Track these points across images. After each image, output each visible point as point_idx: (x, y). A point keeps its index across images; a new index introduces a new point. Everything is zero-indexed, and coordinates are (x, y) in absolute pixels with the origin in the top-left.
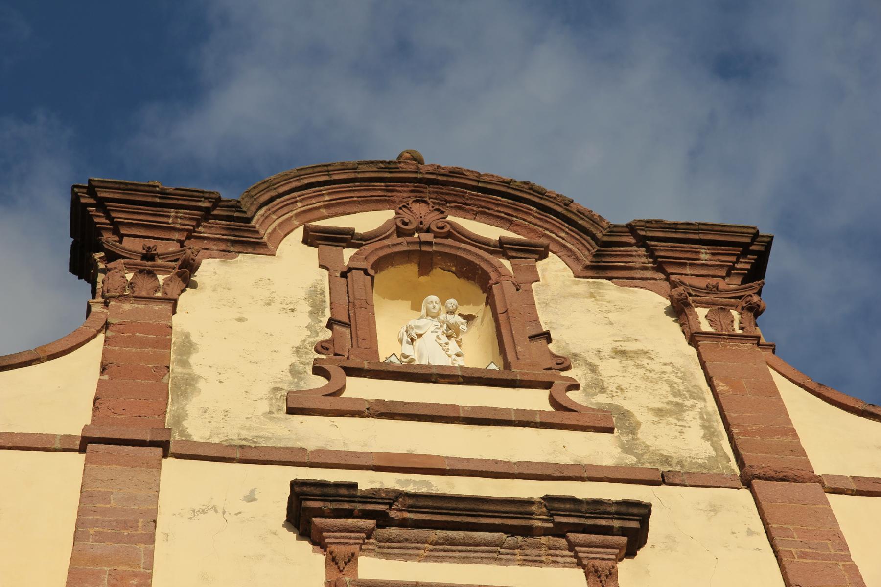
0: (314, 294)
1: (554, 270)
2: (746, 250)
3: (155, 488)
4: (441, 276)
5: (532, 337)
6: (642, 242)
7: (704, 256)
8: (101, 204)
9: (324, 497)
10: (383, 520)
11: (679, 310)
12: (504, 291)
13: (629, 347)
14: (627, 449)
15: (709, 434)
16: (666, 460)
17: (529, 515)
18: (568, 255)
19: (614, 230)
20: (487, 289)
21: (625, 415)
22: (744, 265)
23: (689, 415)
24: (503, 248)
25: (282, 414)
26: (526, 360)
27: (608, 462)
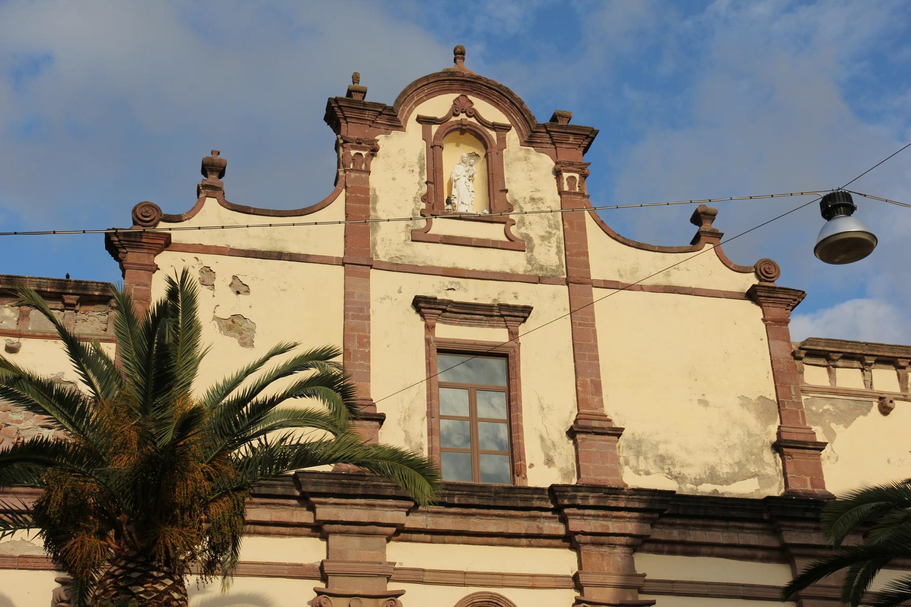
0: (421, 158)
1: (513, 137)
2: (588, 136)
3: (368, 288)
5: (501, 191)
6: (548, 132)
7: (571, 140)
8: (340, 107)
9: (426, 302)
10: (444, 311)
11: (558, 174)
13: (537, 195)
14: (529, 262)
16: (541, 268)
17: (492, 311)
18: (519, 130)
19: (538, 126)
20: (486, 147)
21: (530, 240)
22: (586, 143)
23: (553, 239)
24: (495, 127)
25: (409, 242)
26: (498, 207)
27: (521, 271)
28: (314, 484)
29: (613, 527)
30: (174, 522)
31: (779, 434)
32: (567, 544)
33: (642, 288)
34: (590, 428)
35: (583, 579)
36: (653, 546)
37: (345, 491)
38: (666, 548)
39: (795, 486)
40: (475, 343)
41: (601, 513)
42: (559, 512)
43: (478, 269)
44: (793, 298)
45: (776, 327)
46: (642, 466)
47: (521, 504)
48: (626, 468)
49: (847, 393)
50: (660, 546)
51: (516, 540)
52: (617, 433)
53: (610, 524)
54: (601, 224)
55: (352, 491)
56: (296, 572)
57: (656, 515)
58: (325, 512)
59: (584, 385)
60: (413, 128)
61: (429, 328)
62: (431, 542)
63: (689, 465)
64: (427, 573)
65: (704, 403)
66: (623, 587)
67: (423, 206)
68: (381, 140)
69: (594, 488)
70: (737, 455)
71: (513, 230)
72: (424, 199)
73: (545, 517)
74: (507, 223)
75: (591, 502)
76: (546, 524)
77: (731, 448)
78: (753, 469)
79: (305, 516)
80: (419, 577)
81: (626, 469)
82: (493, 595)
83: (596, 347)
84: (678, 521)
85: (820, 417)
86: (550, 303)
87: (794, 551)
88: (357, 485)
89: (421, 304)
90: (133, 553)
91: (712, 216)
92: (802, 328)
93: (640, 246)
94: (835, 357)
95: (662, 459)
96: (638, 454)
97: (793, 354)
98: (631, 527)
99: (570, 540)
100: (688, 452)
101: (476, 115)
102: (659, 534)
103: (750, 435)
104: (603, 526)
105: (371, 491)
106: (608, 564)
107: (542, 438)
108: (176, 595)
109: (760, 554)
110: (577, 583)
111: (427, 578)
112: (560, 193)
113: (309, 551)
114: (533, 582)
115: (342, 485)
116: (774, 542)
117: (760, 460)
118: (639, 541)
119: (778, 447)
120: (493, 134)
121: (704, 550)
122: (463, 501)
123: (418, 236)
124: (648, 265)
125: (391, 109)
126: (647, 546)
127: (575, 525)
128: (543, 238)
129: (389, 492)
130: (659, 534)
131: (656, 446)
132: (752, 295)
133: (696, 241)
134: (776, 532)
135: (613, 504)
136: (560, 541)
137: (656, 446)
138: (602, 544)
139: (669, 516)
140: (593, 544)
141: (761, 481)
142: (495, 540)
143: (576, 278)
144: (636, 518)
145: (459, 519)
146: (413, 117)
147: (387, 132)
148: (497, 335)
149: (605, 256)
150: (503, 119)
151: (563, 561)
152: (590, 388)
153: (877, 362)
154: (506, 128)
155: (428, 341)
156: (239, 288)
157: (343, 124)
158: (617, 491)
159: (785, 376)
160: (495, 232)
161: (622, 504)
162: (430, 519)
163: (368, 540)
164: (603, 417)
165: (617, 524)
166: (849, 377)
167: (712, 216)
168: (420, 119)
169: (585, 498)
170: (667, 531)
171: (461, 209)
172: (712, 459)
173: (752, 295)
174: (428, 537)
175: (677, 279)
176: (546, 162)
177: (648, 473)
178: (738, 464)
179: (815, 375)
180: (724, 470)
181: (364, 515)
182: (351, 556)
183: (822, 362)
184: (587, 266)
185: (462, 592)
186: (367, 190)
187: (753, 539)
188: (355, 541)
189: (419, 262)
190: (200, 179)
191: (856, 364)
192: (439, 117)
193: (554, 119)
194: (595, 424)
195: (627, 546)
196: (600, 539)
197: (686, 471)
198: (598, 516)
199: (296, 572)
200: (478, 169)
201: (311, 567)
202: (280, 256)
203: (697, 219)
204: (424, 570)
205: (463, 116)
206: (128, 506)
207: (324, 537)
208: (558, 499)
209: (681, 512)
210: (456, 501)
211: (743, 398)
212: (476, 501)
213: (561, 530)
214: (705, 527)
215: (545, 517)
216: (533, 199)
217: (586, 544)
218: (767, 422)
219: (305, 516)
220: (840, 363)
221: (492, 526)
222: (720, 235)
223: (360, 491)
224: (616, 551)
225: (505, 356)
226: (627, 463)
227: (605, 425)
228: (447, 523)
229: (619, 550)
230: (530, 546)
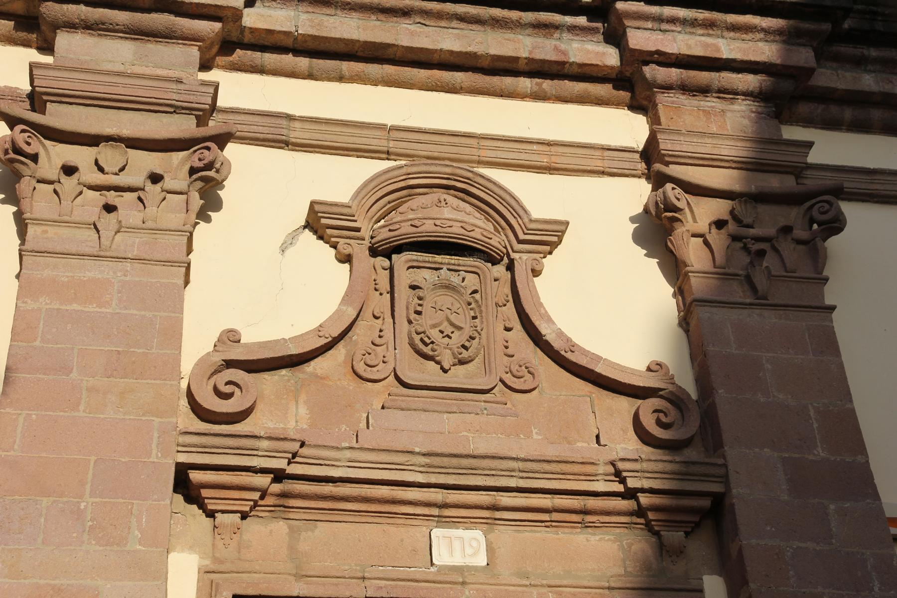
29: (727, 47)
32: (625, 95)
35: (666, 144)
36: (817, 109)
38: (848, 114)
50: (834, 110)
51: (508, 82)
53: (721, 43)
57: (826, 27)
62: (310, 76)
64: (297, 125)
73: (572, 29)
76: (575, 45)
80: (277, 133)
84: (874, 53)
98: (765, 51)
99: (630, 85)
102: (830, 78)
104: (706, 45)
110: (650, 153)
111: (297, 134)
118: (787, 86)
126: (804, 108)
127: (640, 39)
130: (830, 78)
136: (610, 86)
138: (704, 91)
139: (852, 37)
140: (686, 88)
144: (779, 32)
162: (304, 16)
165: (738, 44)
170: (848, 75)
174: (303, 63)
198: (693, 23)
204: (290, 118)
209: (879, 26)
213: (610, 57)
215: (572, 29)
217: (667, 87)
224: (736, 107)
230: (539, 96)
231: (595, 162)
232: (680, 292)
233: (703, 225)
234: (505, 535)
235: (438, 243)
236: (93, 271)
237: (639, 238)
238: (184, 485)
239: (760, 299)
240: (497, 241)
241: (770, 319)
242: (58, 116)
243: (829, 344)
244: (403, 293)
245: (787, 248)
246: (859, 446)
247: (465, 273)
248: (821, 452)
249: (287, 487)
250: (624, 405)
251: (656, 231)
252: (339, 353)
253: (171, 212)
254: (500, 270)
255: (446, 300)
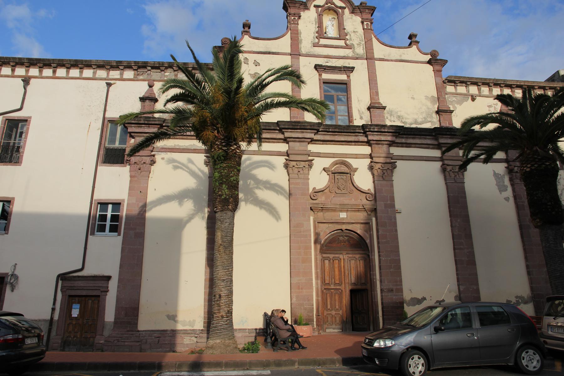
0: (315, 19)
1: (347, 11)
4: (331, 11)
7: (367, 11)
11: (362, 23)
12: (340, 17)
13: (355, 30)
15: (363, 49)
16: (358, 54)
18: (349, 8)
19: (356, 6)
21: (353, 45)
24: (341, 8)
26: (342, 34)
28: (284, 125)
29: (383, 138)
30: (236, 126)
31: (438, 108)
33: (392, 61)
34: (374, 107)
35: (373, 155)
36: (396, 145)
37: (294, 127)
38: (400, 145)
39: (443, 125)
40: (336, 80)
41: (379, 133)
42: (365, 133)
43: (336, 55)
44: (444, 62)
45: (437, 72)
46: (392, 119)
47: (352, 131)
48: (387, 120)
49: (461, 94)
51: (350, 143)
52: (384, 108)
54: (378, 39)
55: (296, 127)
56: (279, 154)
58: (287, 135)
59: (373, 93)
60: (313, 9)
61: (320, 75)
63: (408, 119)
65: (413, 98)
66: (386, 157)
67: (317, 35)
68: (302, 14)
69: (377, 125)
70: (424, 115)
71: (348, 42)
72: (317, 33)
74: (345, 39)
75: (376, 130)
77: (422, 113)
78: (429, 120)
79: (281, 136)
80: (319, 155)
81: (387, 120)
82: (343, 161)
83: (377, 80)
85: (452, 102)
86: (361, 66)
87: (442, 145)
88: (298, 125)
89: (317, 67)
90: (222, 138)
91: (415, 36)
92: (447, 72)
93: (391, 47)
94: (457, 82)
95: (399, 117)
96: (391, 115)
97: (443, 81)
99: (369, 143)
100: (408, 114)
101: (334, 4)
102: (398, 140)
103: (428, 108)
105: (302, 127)
106: (381, 151)
107: (359, 111)
108: (238, 151)
109: (431, 146)
110: (371, 156)
112: (364, 29)
113: (283, 147)
114: (356, 156)
115: (293, 125)
116: (436, 143)
117: (432, 117)
119: (438, 112)
120: (340, 10)
121: (413, 145)
122: (333, 130)
123: (315, 45)
124: (395, 53)
125: (305, 3)
126: (394, 145)
127: (370, 138)
128: (358, 44)
129: (308, 127)
130: (398, 140)
131: (397, 113)
132: (429, 62)
133: (410, 44)
134: (437, 139)
135: (383, 130)
137: (397, 113)
138: (379, 144)
139: (402, 134)
141: (432, 123)
142: (344, 143)
143: (370, 58)
145: (332, 136)
146: (313, 5)
147: (304, 11)
148: (342, 77)
149: (379, 50)
150: (343, 5)
151: (367, 150)
152: (375, 94)
153: (471, 84)
154: (344, 8)
155: (320, 80)
156: (257, 64)
157: (289, 9)
158: (385, 126)
159: (440, 89)
160: (342, 43)
161: (386, 130)
163: (302, 143)
164: (379, 103)
166: (462, 89)
167: (415, 36)
168: (315, 6)
169: (374, 128)
171: (330, 36)
172: (416, 117)
173: (429, 62)
174: (322, 143)
175: (404, 58)
176: (358, 19)
177: (394, 121)
178: (424, 118)
179: (450, 89)
180: (420, 120)
181: (300, 135)
182: (296, 148)
183: (453, 84)
184: (373, 53)
185: (333, 160)
186: (297, 30)
187: (429, 142)
188: (298, 144)
189: (316, 53)
190: (242, 29)
191: (464, 85)
192: (322, 5)
193: (361, 4)
194: (377, 105)
195: (387, 144)
196: (378, 142)
197: (407, 121)
199: (279, 154)
200: (335, 22)
201: (284, 152)
202: (269, 53)
203: (410, 37)
205: (329, 4)
206: (220, 122)
207: (288, 143)
208: (365, 129)
210: (331, 130)
211: (426, 96)
212: (337, 130)
213: (366, 139)
214: (413, 138)
216: (354, 32)
218: (434, 104)
219: (281, 136)
220: (459, 85)
221: (342, 138)
222: (418, 42)
223: (298, 127)
225: (346, 84)
226: (387, 118)
227: (380, 105)
228: (328, 138)
229: (385, 146)
231: (363, 156)
232: (373, 177)
233: (377, 168)
234: (349, 213)
235: (341, 173)
236: (298, 181)
237: (368, 169)
238: (311, 209)
239: (384, 179)
240: (348, 172)
241: (385, 182)
242: (292, 157)
243: (392, 186)
244: (336, 179)
245: (388, 171)
246: (394, 201)
247: (344, 176)
248: (389, 202)
249: (322, 209)
250: (365, 195)
251: (371, 168)
252: (328, 189)
253: (306, 171)
254: (349, 175)
255: (341, 180)
